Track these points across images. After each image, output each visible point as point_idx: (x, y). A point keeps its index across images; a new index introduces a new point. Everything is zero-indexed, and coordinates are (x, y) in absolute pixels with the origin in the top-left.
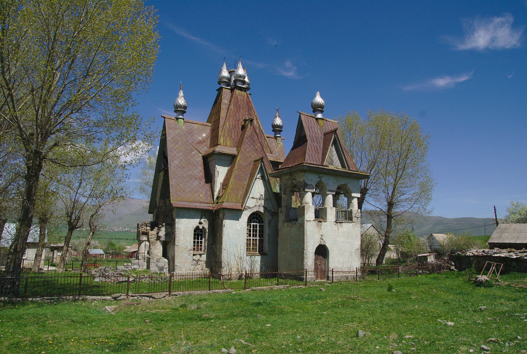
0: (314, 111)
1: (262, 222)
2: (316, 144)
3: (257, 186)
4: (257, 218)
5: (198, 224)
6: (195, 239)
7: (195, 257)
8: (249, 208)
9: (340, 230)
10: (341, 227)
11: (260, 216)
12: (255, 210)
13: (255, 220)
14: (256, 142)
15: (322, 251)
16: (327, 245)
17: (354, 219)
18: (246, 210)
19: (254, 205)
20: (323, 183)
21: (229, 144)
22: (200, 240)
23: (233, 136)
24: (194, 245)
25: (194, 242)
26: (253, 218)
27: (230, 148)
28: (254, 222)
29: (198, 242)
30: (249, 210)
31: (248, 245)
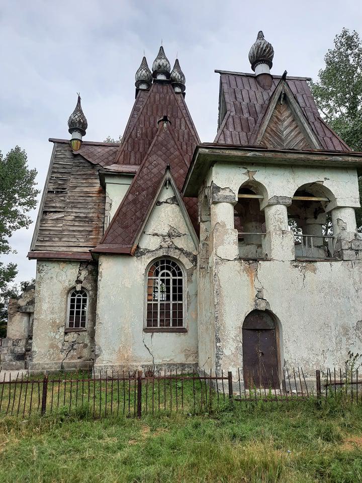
0: (253, 68)
1: (180, 274)
2: (246, 115)
3: (163, 215)
4: (169, 268)
5: (74, 284)
6: (72, 307)
7: (67, 338)
8: (149, 251)
9: (307, 278)
10: (314, 270)
11: (174, 264)
12: (161, 253)
13: (165, 271)
14: (172, 150)
15: (261, 326)
16: (275, 310)
17: (347, 254)
18: (143, 254)
19: (158, 246)
20: (259, 184)
21: (132, 160)
22: (75, 310)
23: (141, 149)
24: (71, 318)
25: (72, 313)
26: (162, 268)
27: (128, 166)
28: (163, 275)
29: (78, 313)
30: (150, 254)
31: (151, 311)
